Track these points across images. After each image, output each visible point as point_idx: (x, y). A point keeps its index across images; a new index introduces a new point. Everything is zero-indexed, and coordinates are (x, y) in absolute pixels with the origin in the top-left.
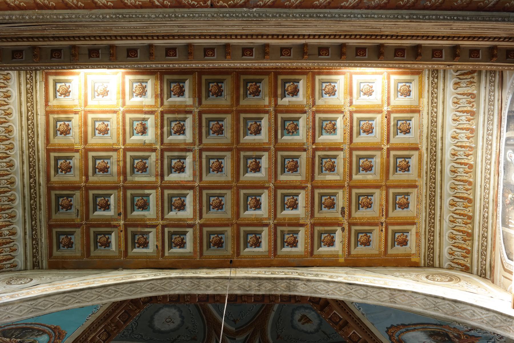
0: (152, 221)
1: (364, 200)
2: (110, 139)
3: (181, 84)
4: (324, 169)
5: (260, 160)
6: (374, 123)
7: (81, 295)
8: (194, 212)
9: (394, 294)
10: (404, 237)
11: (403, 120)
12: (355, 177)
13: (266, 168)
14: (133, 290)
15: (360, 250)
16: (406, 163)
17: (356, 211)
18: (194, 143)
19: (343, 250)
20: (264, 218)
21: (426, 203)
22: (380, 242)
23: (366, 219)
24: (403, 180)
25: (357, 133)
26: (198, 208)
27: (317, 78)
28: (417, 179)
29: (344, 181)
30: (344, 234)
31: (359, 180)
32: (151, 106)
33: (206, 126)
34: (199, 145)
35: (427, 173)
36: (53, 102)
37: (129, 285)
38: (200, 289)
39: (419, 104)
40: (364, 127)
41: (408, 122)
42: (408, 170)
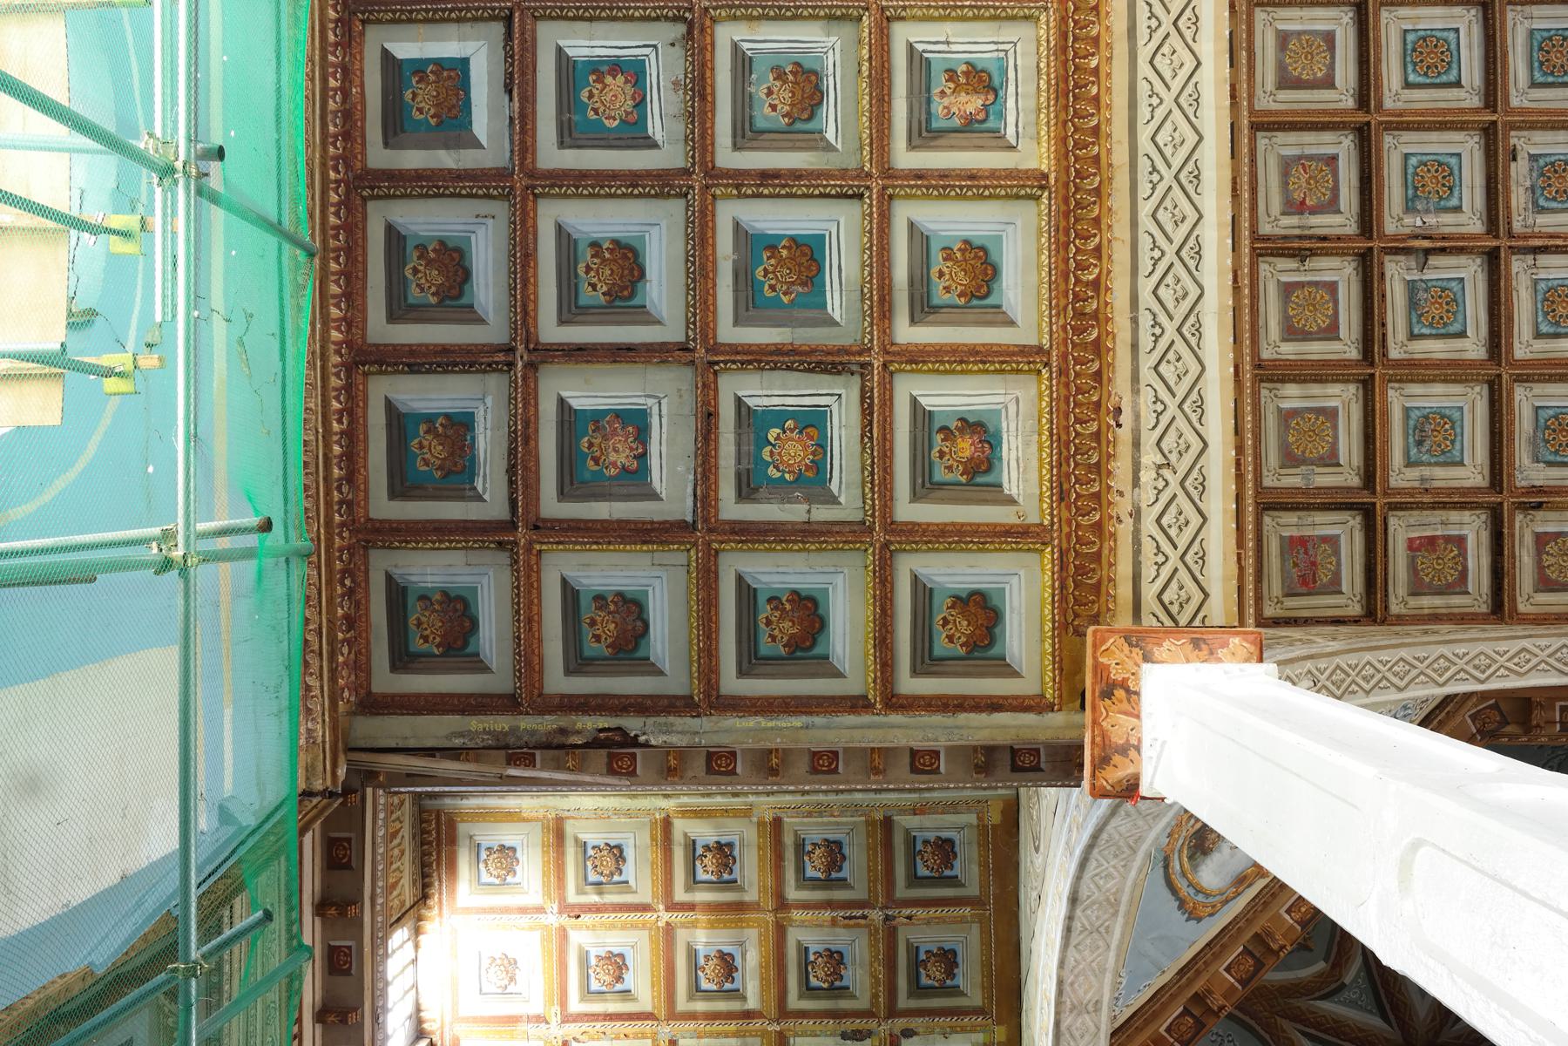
1: (821, 974)
6: (593, 952)
9: (1073, 1004)
10: (929, 849)
11: (585, 866)
12: (752, 1003)
15: (970, 981)
16: (708, 854)
17: (853, 997)
19: (971, 1031)
21: (825, 792)
22: (944, 922)
23: (876, 965)
24: (760, 860)
25: (624, 1000)
28: (755, 819)
29: (764, 1034)
30: (921, 1030)
31: (762, 990)
35: (735, 795)
39: (537, 820)
40: (608, 979)
41: (591, 852)
42: (730, 845)
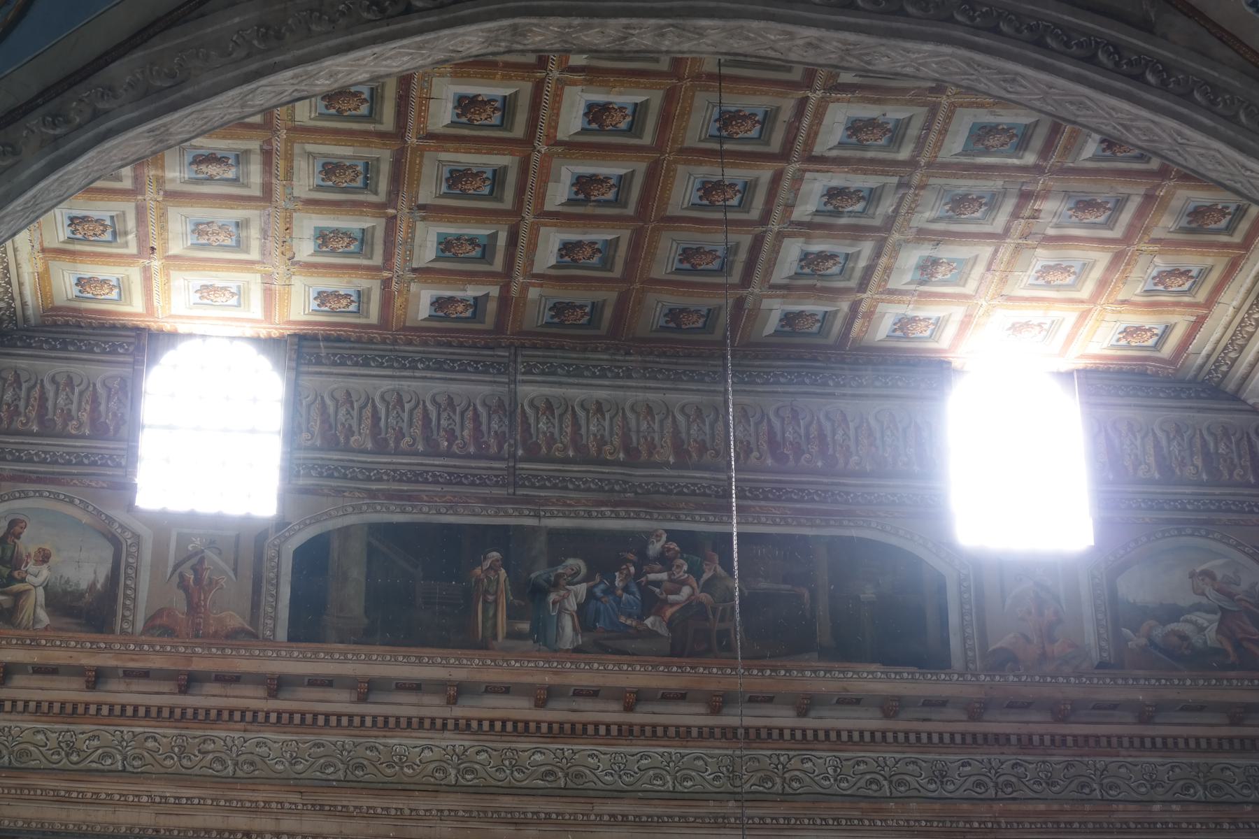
0: (974, 103)
2: (1043, 256)
3: (787, 329)
4: (360, 168)
5: (574, 197)
7: (1228, 176)
8: (823, 114)
13: (558, 181)
14: (1072, 103)
18: (780, 236)
20: (582, 84)
26: (806, 122)
27: (374, 316)
29: (290, 142)
32: (890, 302)
33: (733, 262)
34: (765, 232)
36: (1181, 322)
37: (1079, 120)
38: (845, 43)
